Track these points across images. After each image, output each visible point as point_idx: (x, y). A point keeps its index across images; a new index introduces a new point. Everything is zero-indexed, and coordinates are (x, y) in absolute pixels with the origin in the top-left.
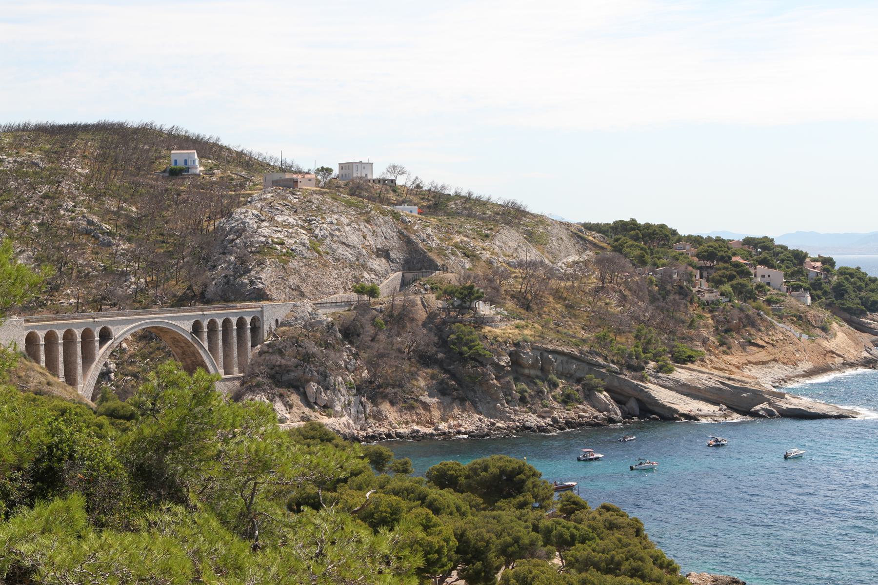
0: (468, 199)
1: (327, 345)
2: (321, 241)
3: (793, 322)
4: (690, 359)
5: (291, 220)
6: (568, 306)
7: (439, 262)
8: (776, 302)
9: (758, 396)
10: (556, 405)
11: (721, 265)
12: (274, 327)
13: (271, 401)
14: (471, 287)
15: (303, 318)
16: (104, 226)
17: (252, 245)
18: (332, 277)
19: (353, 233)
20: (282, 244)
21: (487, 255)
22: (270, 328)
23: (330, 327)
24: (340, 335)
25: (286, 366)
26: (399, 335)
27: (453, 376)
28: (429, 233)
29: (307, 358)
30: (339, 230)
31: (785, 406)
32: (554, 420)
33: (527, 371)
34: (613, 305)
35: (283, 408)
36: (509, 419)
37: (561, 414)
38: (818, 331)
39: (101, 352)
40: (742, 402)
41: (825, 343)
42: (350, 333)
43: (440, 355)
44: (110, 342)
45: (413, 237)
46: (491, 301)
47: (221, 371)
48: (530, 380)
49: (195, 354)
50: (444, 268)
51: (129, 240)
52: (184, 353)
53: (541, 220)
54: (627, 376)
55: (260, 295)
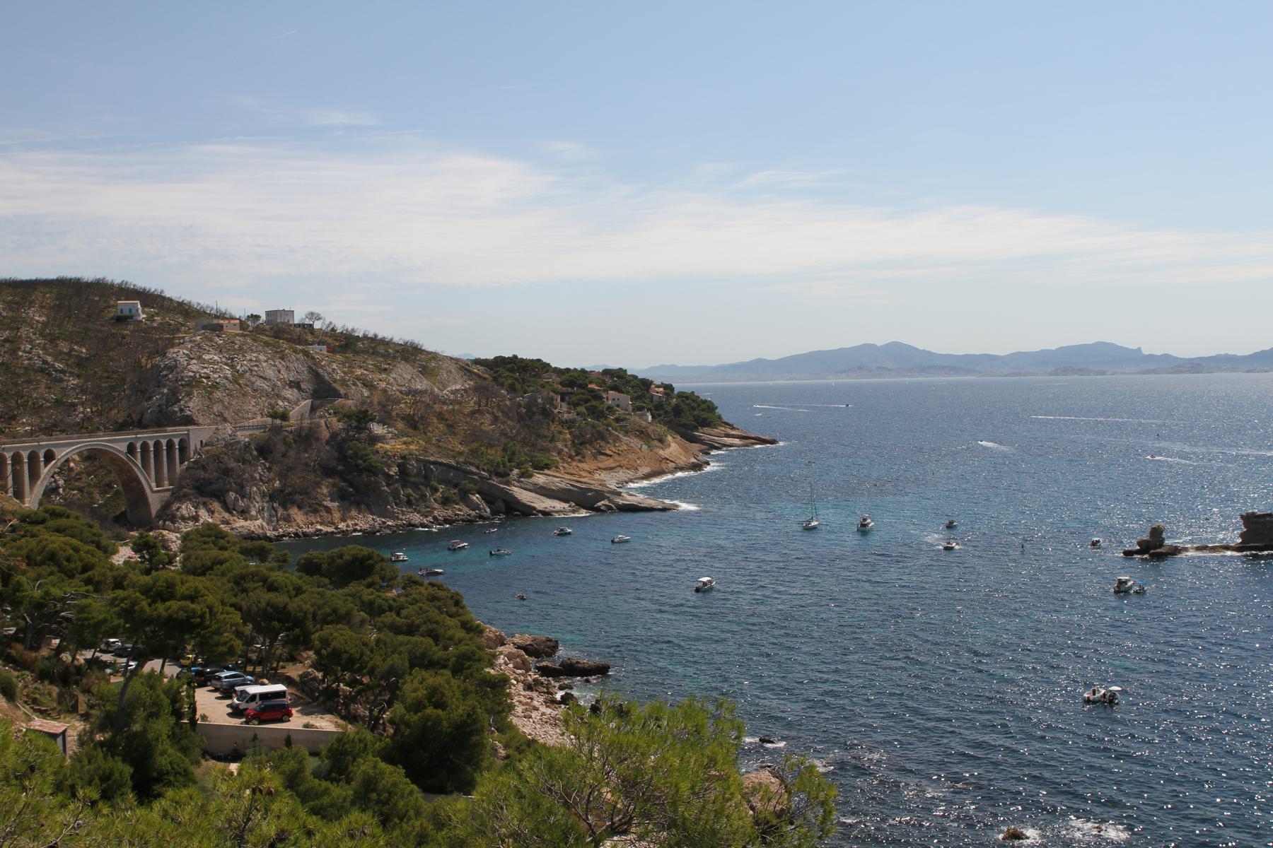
0: (374, 340)
1: (244, 461)
2: (242, 376)
3: (636, 436)
4: (547, 467)
6: (448, 426)
7: (342, 392)
8: (623, 420)
9: (600, 495)
10: (436, 505)
11: (580, 391)
14: (366, 411)
16: (57, 365)
17: (182, 379)
18: (251, 405)
19: (268, 368)
20: (208, 378)
21: (383, 385)
23: (247, 446)
24: (255, 453)
26: (306, 451)
27: (351, 484)
28: (334, 369)
29: (227, 472)
31: (621, 502)
32: (435, 518)
33: (412, 479)
34: (486, 423)
36: (398, 518)
37: (440, 513)
38: (656, 443)
39: (45, 471)
40: (586, 499)
41: (661, 452)
42: (264, 450)
43: (340, 468)
45: (320, 371)
46: (382, 422)
47: (153, 484)
48: (415, 486)
50: (346, 397)
51: (79, 376)
53: (434, 356)
54: (495, 481)
55: (189, 421)
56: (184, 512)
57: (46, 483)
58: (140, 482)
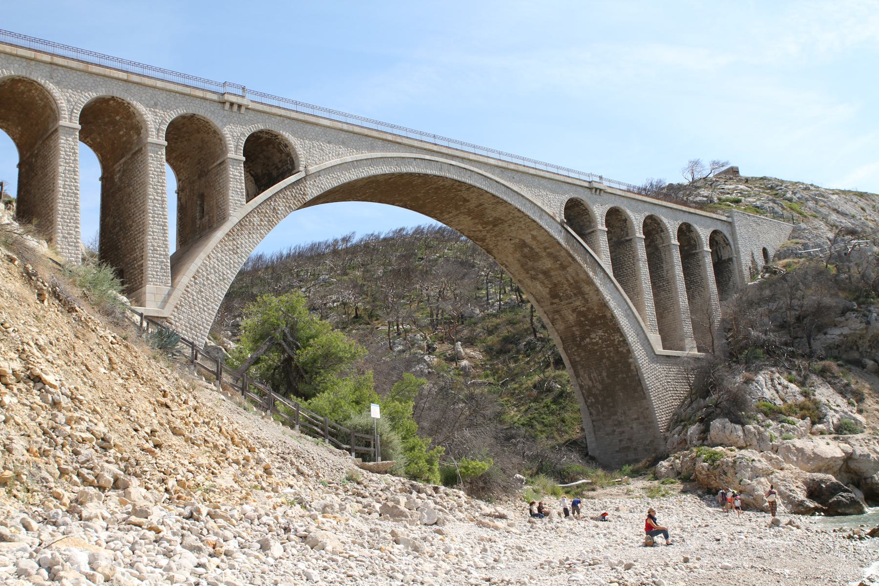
12: (761, 263)
13: (802, 384)
15: (819, 246)
22: (753, 261)
25: (820, 310)
30: (823, 196)
35: (839, 400)
47: (655, 339)
49: (581, 286)
52: (554, 295)
56: (768, 394)
58: (616, 329)
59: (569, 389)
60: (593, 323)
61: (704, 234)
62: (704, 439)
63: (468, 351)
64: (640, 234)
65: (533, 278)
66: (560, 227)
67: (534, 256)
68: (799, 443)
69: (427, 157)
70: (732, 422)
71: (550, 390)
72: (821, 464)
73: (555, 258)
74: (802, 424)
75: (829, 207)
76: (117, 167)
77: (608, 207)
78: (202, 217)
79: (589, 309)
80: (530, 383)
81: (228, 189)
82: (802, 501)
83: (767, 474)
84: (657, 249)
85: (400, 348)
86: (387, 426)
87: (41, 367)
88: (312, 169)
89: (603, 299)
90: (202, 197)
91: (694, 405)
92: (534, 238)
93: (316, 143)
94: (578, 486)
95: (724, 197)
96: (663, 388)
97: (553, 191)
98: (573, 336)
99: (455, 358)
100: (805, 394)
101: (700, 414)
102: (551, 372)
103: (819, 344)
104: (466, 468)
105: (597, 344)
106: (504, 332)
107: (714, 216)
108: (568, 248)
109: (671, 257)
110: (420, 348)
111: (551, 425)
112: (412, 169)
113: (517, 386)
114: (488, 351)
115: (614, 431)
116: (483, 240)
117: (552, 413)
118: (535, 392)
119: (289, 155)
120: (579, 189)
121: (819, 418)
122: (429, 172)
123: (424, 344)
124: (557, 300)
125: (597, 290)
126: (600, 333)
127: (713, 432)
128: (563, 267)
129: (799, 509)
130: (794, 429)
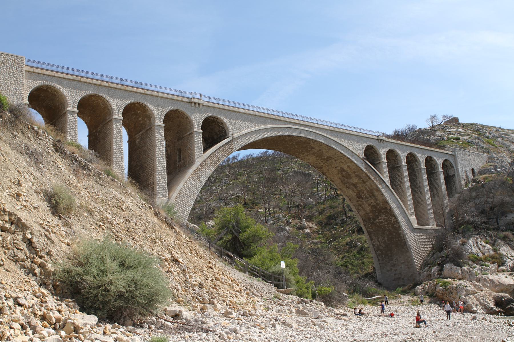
5: (460, 130)
12: (471, 176)
13: (493, 245)
15: (503, 167)
22: (467, 176)
25: (503, 204)
30: (507, 135)
44: (225, 141)
49: (374, 192)
52: (359, 196)
56: (475, 250)
57: (206, 175)
58: (393, 215)
59: (366, 246)
60: (380, 211)
61: (439, 162)
62: (441, 274)
63: (309, 224)
64: (405, 163)
65: (348, 188)
66: (362, 161)
67: (348, 176)
68: (491, 277)
69: (293, 127)
70: (455, 265)
71: (355, 246)
72: (502, 288)
73: (360, 177)
74: (493, 267)
75: (510, 141)
76: (137, 136)
77: (387, 149)
78: (180, 161)
79: (378, 204)
80: (344, 242)
81: (194, 148)
82: (492, 308)
83: (474, 293)
84: (414, 170)
85: (272, 222)
86: (288, 271)
87: (177, 256)
88: (236, 135)
89: (386, 199)
90: (180, 150)
91: (435, 256)
92: (348, 167)
93: (237, 122)
94: (374, 299)
95: (450, 136)
96: (418, 246)
97: (358, 142)
98: (369, 219)
99: (302, 228)
100: (495, 250)
101: (438, 261)
102: (355, 236)
103: (503, 221)
104: (321, 291)
105: (382, 222)
106: (328, 213)
107: (445, 152)
108: (367, 172)
109: (422, 175)
110: (282, 222)
111: (357, 266)
112: (286, 133)
113: (337, 243)
114: (320, 223)
115: (392, 269)
116: (321, 168)
117: (357, 259)
118: (347, 247)
119: (223, 128)
120: (372, 140)
121: (503, 264)
122: (294, 134)
123: (285, 220)
124: (360, 199)
125: (382, 194)
126: (384, 217)
127: (445, 271)
128: (364, 182)
129: (490, 311)
130: (488, 269)
